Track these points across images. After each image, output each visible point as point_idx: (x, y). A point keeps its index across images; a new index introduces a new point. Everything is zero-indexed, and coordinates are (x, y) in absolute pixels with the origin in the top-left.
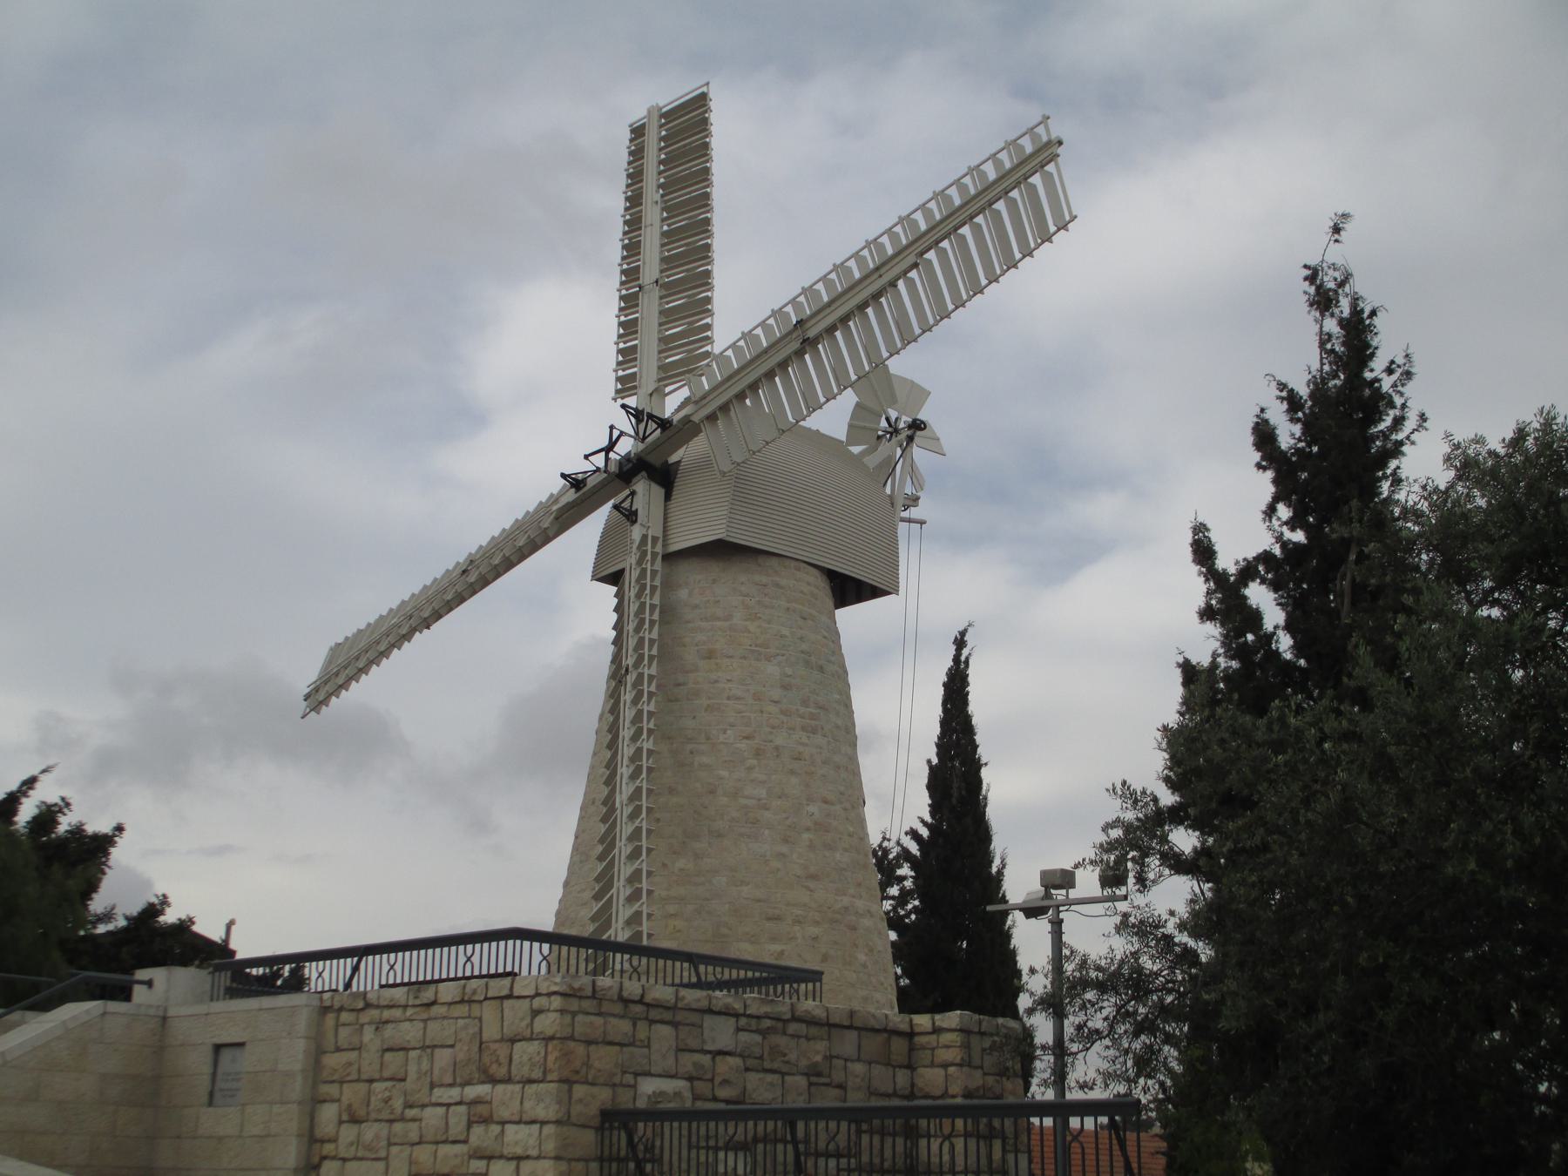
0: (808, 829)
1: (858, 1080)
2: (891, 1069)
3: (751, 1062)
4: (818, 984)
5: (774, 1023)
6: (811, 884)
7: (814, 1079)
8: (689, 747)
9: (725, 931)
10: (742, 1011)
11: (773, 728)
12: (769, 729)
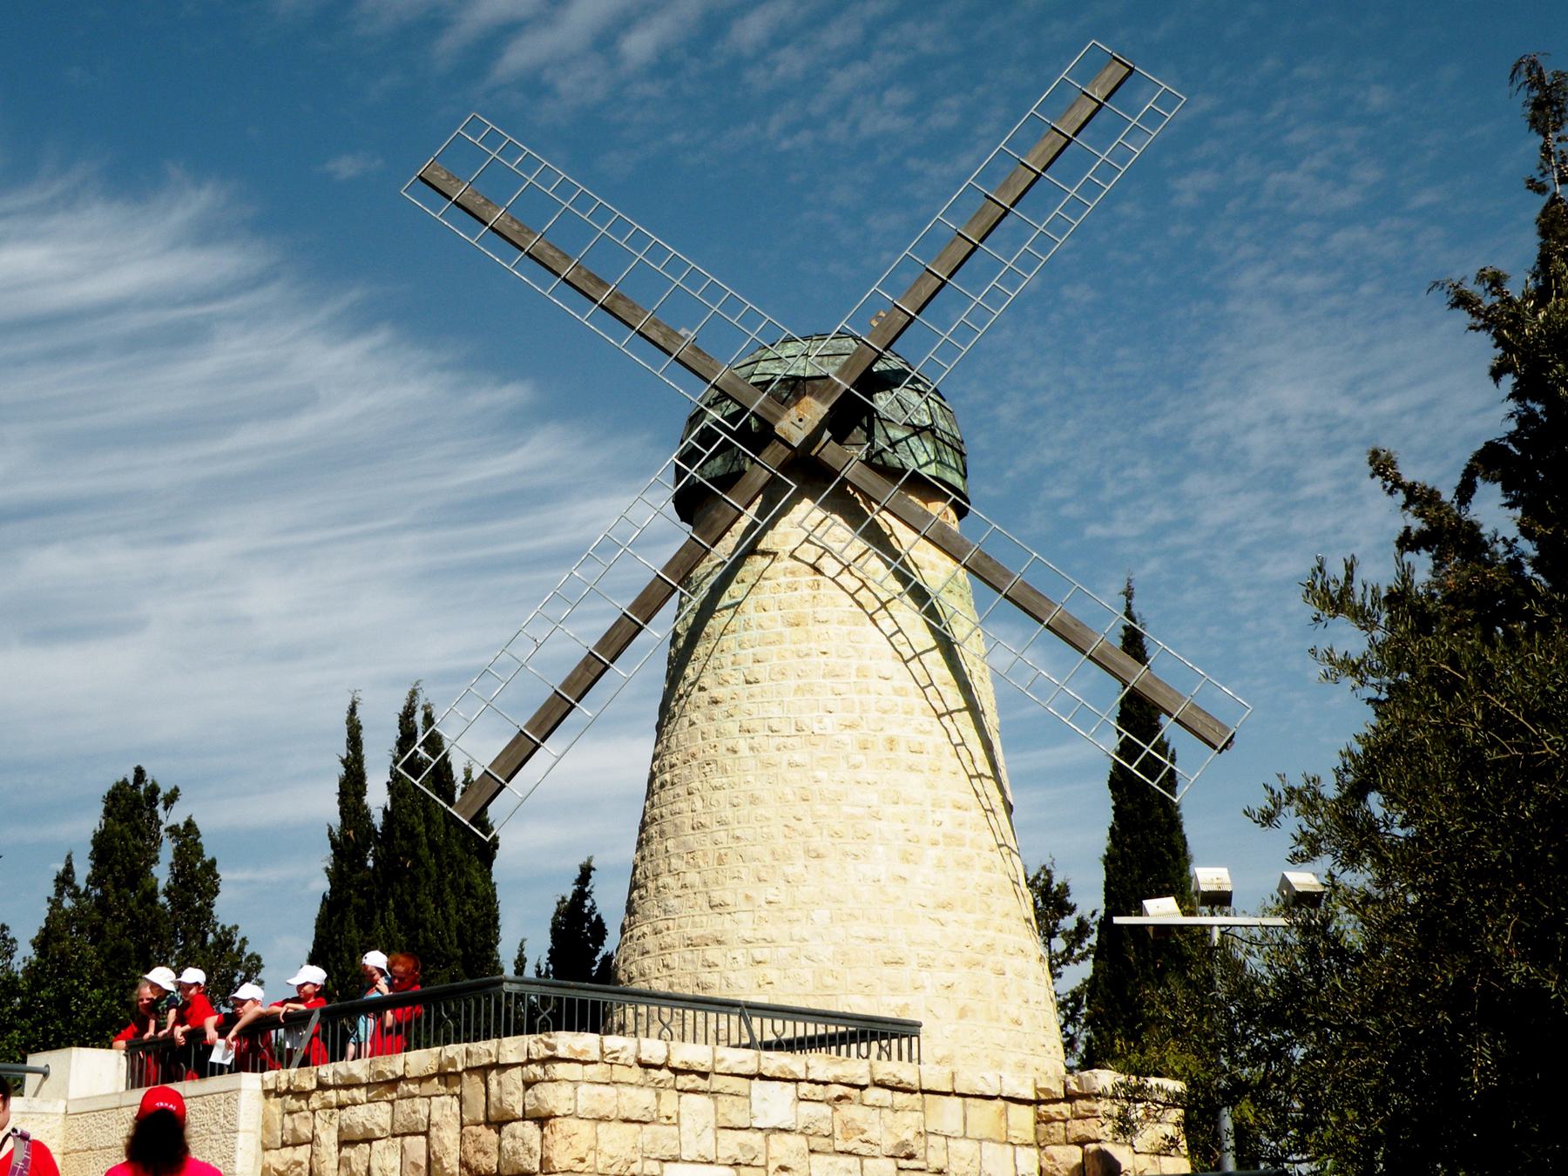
0: (935, 844)
1: (964, 1163)
2: (1009, 1148)
3: (817, 1143)
4: (915, 1040)
5: (846, 1090)
6: (943, 915)
7: (904, 1163)
9: (829, 981)
10: (802, 1076)
12: (879, 714)
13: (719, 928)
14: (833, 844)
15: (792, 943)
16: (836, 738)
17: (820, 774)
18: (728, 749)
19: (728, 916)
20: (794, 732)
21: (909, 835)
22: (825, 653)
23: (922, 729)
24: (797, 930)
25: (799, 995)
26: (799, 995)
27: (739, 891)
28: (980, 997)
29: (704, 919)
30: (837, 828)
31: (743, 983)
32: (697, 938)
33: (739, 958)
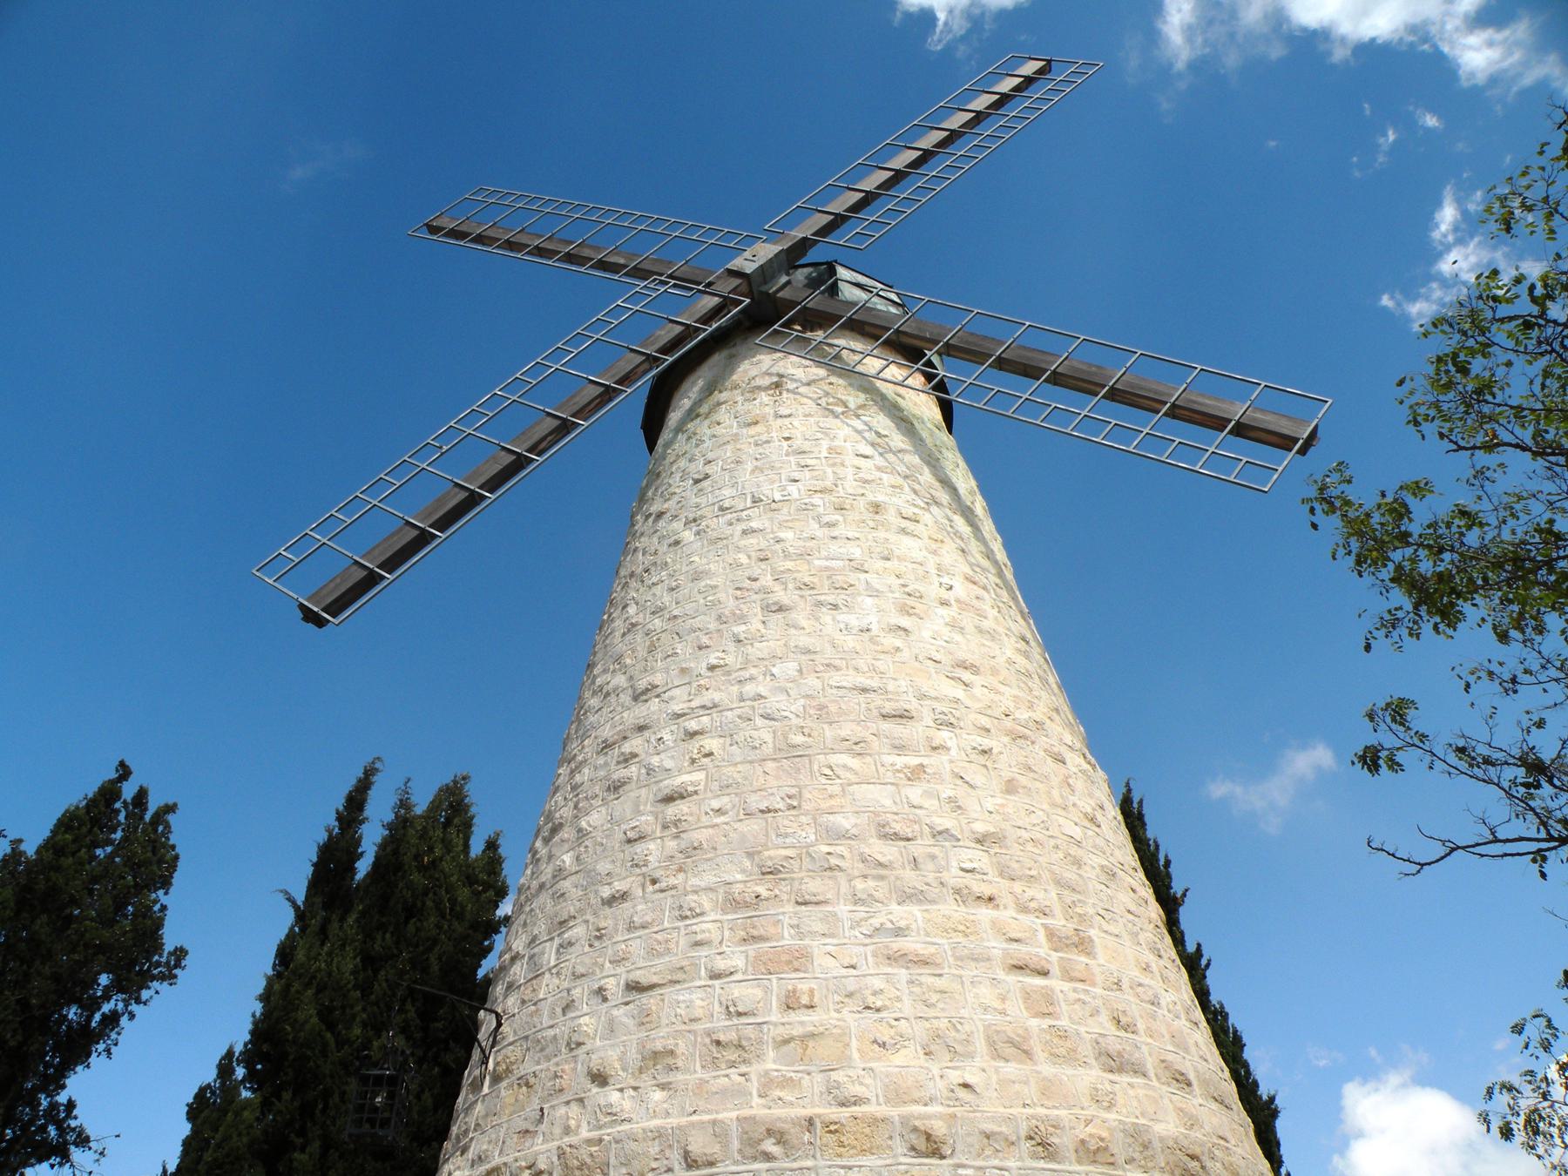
9: (798, 739)
11: (866, 482)
14: (802, 597)
15: (742, 704)
16: (807, 501)
22: (788, 439)
24: (749, 689)
25: (751, 762)
26: (751, 762)
30: (807, 580)
31: (669, 764)
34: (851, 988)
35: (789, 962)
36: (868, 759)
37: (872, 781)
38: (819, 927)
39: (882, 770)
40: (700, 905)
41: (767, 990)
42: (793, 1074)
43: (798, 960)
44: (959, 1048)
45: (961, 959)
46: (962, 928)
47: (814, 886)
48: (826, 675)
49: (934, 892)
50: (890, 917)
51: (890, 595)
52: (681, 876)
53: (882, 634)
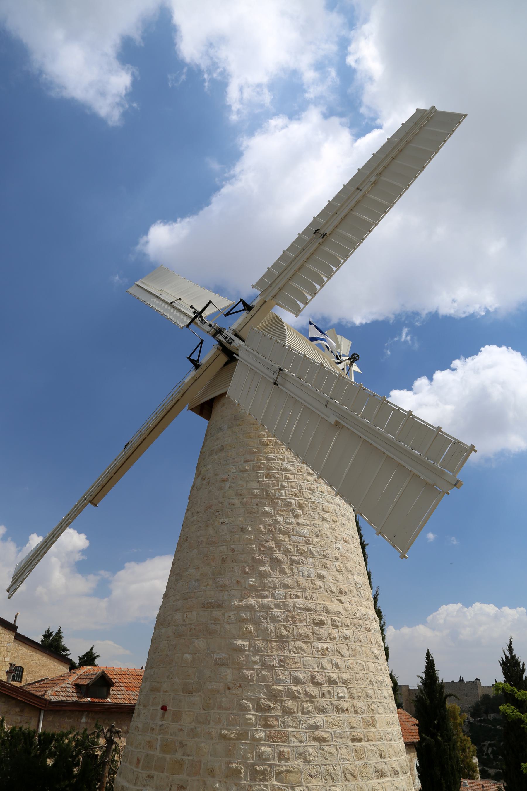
6: (343, 598)
8: (255, 501)
9: (285, 632)
13: (220, 598)
17: (280, 519)
18: (229, 504)
19: (226, 592)
20: (265, 496)
21: (325, 553)
22: (281, 459)
23: (328, 500)
27: (234, 578)
28: (361, 644)
29: (212, 593)
32: (207, 604)
33: (232, 617)
34: (302, 751)
35: (280, 738)
36: (309, 645)
37: (310, 655)
38: (291, 723)
39: (314, 650)
40: (249, 706)
41: (274, 750)
42: (282, 787)
43: (284, 738)
44: (335, 777)
45: (336, 737)
46: (337, 724)
47: (290, 704)
48: (295, 600)
49: (329, 707)
50: (315, 720)
51: (319, 557)
52: (240, 689)
53: (315, 579)
